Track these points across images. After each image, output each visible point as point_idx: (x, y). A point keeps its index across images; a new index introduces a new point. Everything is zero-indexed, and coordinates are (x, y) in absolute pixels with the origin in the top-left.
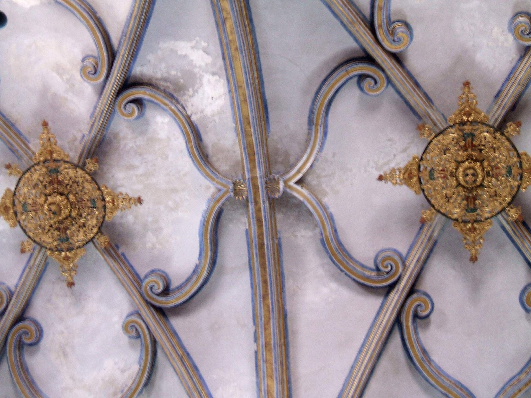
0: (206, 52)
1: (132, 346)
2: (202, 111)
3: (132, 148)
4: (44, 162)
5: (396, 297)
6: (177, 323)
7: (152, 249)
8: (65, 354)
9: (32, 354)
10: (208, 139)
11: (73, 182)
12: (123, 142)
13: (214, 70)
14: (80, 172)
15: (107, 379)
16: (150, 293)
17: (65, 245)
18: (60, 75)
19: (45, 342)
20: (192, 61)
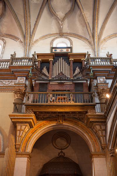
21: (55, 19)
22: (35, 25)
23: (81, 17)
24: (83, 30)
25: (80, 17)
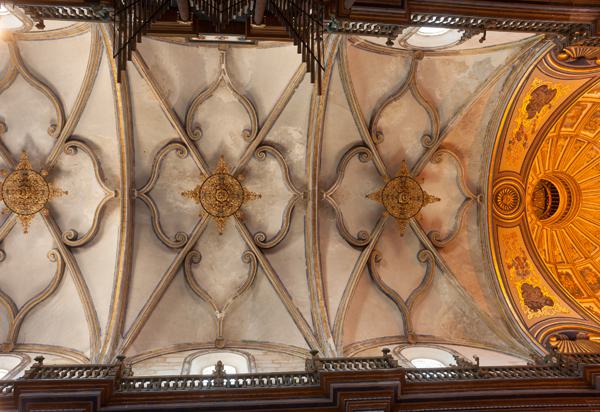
0: (300, 132)
5: (367, 251)
6: (269, 257)
8: (212, 269)
9: (196, 267)
10: (293, 173)
17: (221, 215)
19: (202, 261)
21: (242, 86)
22: (302, 79)
24: (156, 57)
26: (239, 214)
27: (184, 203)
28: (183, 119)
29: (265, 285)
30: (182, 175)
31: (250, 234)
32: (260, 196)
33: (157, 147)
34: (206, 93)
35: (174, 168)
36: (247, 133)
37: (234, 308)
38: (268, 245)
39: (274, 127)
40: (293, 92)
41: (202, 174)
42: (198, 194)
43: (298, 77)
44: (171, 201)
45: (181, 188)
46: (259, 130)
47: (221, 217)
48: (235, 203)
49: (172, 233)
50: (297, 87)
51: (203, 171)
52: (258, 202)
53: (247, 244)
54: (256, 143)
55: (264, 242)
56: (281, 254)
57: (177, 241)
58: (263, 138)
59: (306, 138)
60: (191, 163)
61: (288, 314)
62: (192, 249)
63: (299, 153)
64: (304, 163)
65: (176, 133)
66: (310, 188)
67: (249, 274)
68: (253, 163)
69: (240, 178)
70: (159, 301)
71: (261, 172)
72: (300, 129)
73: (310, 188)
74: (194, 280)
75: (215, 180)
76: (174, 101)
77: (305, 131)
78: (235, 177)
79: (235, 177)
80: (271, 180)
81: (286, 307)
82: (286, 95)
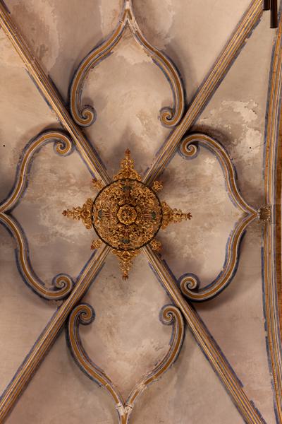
1: (165, 330)
2: (241, 157)
3: (183, 181)
4: (121, 180)
6: (204, 315)
7: (187, 258)
8: (111, 333)
9: (85, 332)
10: (244, 177)
11: (141, 198)
12: (177, 176)
13: (257, 126)
14: (148, 190)
15: (144, 354)
16: (186, 288)
18: (141, 120)
19: (97, 322)
20: (242, 117)
21: (158, 36)
23: (37, 46)
25: (43, 46)
26: (154, 245)
27: (67, 227)
28: (64, 92)
29: (197, 362)
30: (65, 183)
31: (173, 277)
32: (189, 216)
33: (24, 138)
34: (102, 49)
35: (52, 171)
36: (168, 114)
37: (147, 399)
38: (202, 296)
39: (210, 103)
40: (242, 44)
41: (95, 180)
42: (89, 213)
43: (250, 18)
44: (46, 223)
45: (63, 204)
46: (187, 108)
47: (126, 249)
48: (150, 228)
49: (47, 276)
50: (248, 35)
51: (98, 176)
52: (186, 225)
53: (168, 294)
54: (182, 130)
55: (196, 290)
56: (225, 310)
57: (56, 289)
58: (194, 121)
59: (263, 120)
60: (77, 163)
61: (235, 411)
62: (79, 302)
63: (251, 145)
64: (261, 160)
65: (53, 115)
66: (272, 202)
67: (171, 345)
68: (178, 162)
69: (156, 187)
70: (27, 384)
71: (190, 177)
72: (255, 105)
73: (272, 202)
74: (84, 353)
75: (116, 189)
76: (50, 64)
77: (262, 109)
78: (148, 185)
79: (148, 185)
80: (207, 189)
81: (233, 399)
82: (231, 49)
